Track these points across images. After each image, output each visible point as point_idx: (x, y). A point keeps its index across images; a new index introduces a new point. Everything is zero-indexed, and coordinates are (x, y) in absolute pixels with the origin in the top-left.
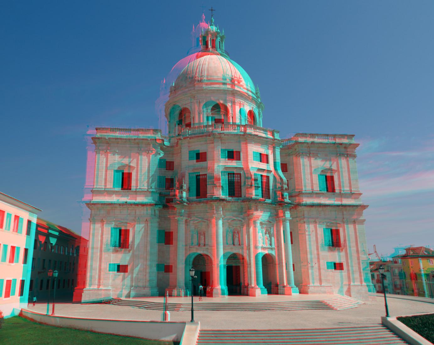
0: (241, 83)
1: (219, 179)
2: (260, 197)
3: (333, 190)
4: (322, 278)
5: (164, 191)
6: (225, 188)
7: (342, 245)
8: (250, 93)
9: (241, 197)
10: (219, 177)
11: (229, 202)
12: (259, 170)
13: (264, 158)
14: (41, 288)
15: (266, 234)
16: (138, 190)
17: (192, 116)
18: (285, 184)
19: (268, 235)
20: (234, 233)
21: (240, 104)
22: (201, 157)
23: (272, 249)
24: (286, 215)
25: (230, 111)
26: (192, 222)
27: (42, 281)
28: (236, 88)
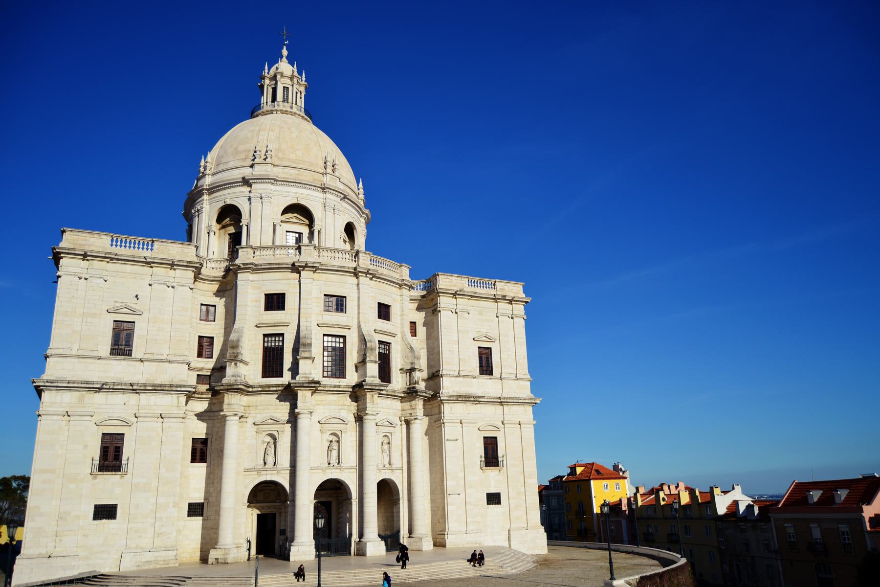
0: (337, 174)
1: (310, 345)
2: (377, 381)
3: (491, 373)
10: (308, 341)
11: (325, 386)
13: (384, 311)
16: (146, 357)
19: (386, 447)
22: (275, 302)
24: (418, 411)
26: (250, 421)
28: (328, 180)
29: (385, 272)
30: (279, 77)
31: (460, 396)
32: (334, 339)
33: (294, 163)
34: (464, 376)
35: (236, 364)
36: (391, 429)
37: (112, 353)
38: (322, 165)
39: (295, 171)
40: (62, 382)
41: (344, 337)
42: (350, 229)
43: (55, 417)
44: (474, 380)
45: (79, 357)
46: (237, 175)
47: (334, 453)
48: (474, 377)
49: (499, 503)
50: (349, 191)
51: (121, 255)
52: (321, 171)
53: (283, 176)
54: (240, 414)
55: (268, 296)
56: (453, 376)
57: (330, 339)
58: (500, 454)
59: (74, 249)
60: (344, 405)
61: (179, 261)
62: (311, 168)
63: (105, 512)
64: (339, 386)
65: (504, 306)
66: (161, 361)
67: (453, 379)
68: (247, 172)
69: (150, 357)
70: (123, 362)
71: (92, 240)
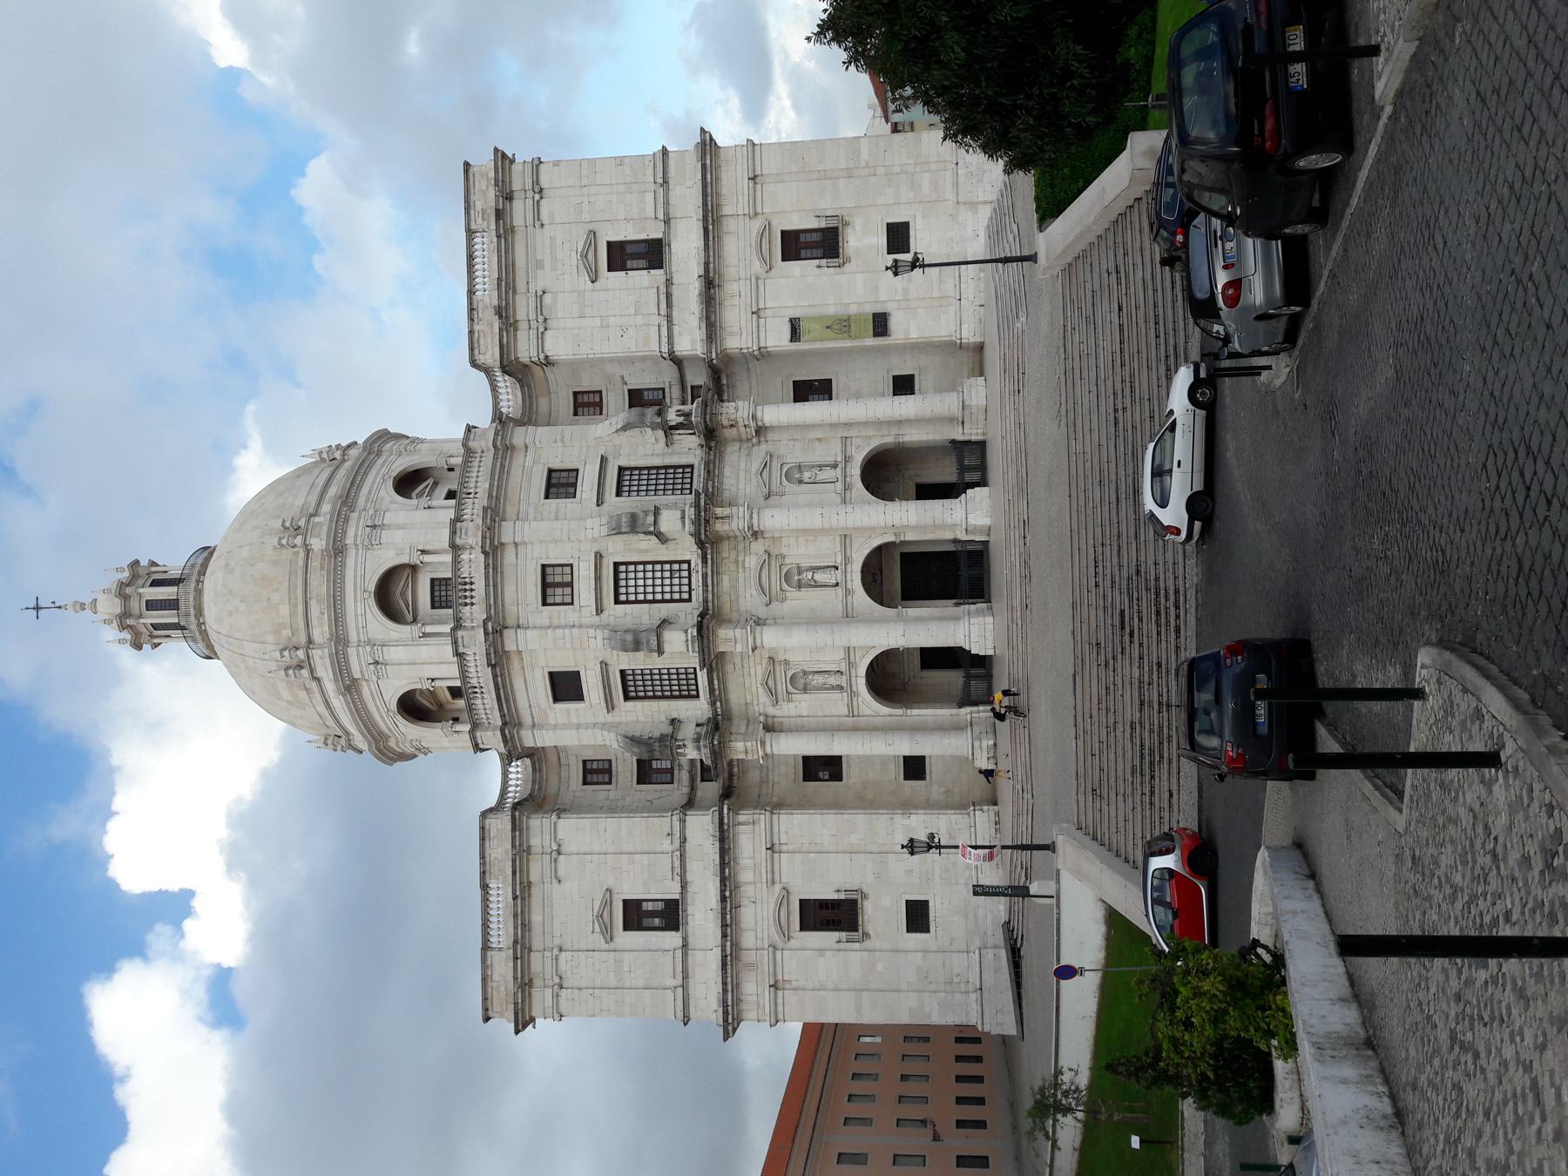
0: (302, 523)
4: (936, 294)
5: (677, 792)
6: (664, 615)
7: (832, 223)
8: (333, 491)
9: (689, 562)
10: (629, 638)
11: (706, 601)
12: (600, 502)
13: (560, 484)
14: (981, 1124)
15: (801, 482)
17: (427, 685)
18: (643, 415)
19: (807, 475)
20: (800, 586)
21: (375, 527)
23: (847, 460)
25: (404, 560)
26: (771, 711)
27: (961, 1124)
29: (484, 485)
30: (130, 622)
31: (708, 318)
32: (623, 583)
33: (296, 605)
34: (669, 305)
35: (679, 747)
36: (776, 465)
37: (676, 929)
38: (287, 554)
39: (313, 604)
40: (725, 1001)
41: (616, 565)
42: (408, 483)
43: (780, 1001)
44: (675, 280)
45: (685, 977)
46: (338, 703)
47: (819, 577)
48: (669, 282)
49: (907, 224)
50: (333, 491)
51: (516, 934)
52: (302, 554)
53: (326, 628)
54: (761, 732)
55: (558, 697)
56: (670, 329)
57: (623, 590)
58: (814, 224)
59: (516, 1004)
60: (737, 561)
61: (513, 846)
62: (300, 573)
63: (917, 916)
64: (705, 576)
65: (520, 211)
66: (682, 856)
67: (676, 330)
68: (330, 686)
69: (678, 870)
70: (690, 910)
71: (496, 977)
